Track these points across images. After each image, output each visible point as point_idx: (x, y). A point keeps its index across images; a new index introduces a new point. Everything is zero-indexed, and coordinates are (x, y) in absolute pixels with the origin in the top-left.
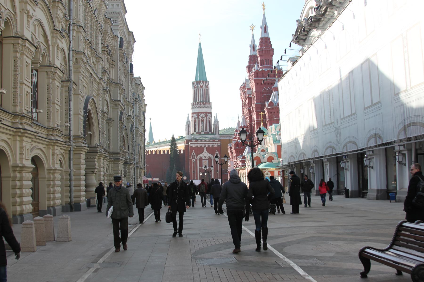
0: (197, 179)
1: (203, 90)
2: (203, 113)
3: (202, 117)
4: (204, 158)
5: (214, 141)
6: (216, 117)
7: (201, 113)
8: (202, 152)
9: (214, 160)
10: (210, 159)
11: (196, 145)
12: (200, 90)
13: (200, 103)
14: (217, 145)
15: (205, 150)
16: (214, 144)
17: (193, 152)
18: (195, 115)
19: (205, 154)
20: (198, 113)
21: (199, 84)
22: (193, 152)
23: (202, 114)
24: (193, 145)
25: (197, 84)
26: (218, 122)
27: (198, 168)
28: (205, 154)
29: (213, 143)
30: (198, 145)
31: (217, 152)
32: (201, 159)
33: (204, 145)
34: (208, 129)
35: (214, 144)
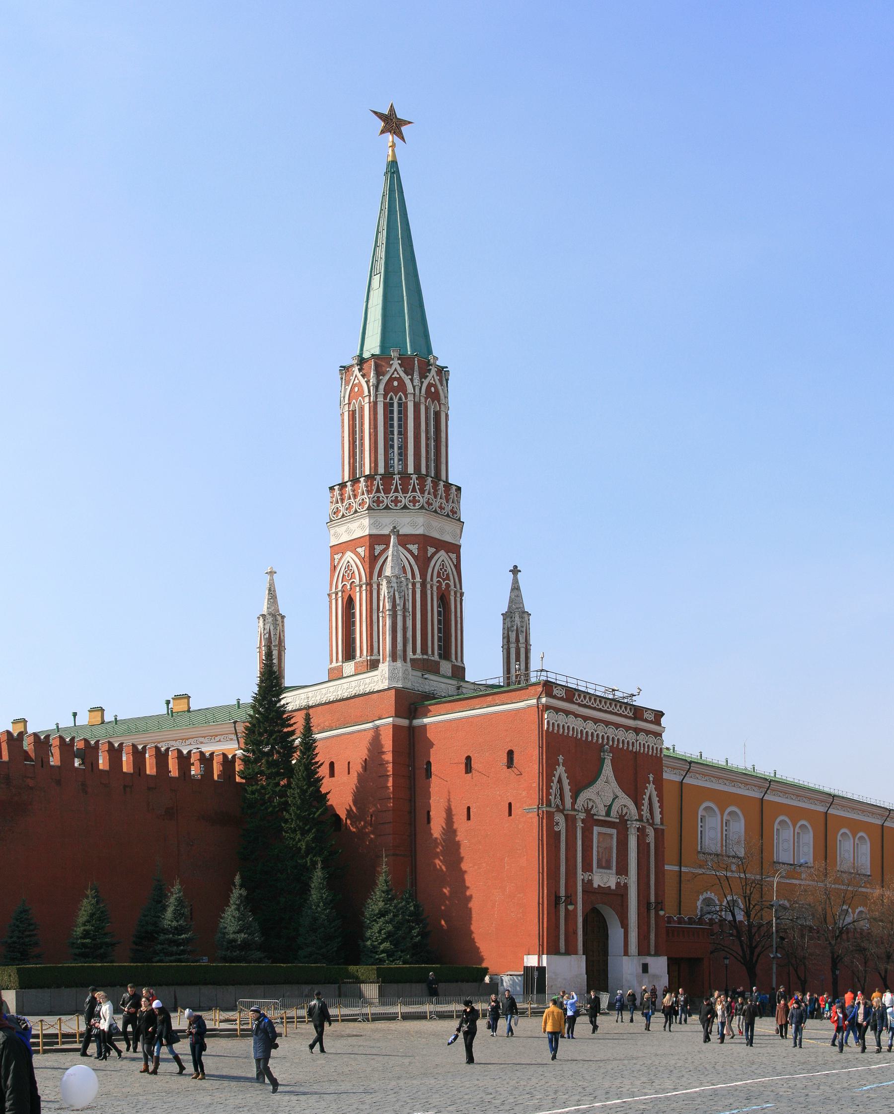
1: (437, 415)
6: (516, 588)
7: (440, 545)
10: (622, 825)
11: (572, 722)
12: (427, 409)
16: (642, 737)
17: (560, 770)
19: (605, 793)
20: (425, 541)
21: (423, 376)
22: (560, 770)
23: (442, 553)
24: (561, 719)
26: (524, 615)
27: (580, 875)
28: (605, 793)
29: (637, 731)
30: (578, 724)
31: (651, 787)
32: (591, 820)
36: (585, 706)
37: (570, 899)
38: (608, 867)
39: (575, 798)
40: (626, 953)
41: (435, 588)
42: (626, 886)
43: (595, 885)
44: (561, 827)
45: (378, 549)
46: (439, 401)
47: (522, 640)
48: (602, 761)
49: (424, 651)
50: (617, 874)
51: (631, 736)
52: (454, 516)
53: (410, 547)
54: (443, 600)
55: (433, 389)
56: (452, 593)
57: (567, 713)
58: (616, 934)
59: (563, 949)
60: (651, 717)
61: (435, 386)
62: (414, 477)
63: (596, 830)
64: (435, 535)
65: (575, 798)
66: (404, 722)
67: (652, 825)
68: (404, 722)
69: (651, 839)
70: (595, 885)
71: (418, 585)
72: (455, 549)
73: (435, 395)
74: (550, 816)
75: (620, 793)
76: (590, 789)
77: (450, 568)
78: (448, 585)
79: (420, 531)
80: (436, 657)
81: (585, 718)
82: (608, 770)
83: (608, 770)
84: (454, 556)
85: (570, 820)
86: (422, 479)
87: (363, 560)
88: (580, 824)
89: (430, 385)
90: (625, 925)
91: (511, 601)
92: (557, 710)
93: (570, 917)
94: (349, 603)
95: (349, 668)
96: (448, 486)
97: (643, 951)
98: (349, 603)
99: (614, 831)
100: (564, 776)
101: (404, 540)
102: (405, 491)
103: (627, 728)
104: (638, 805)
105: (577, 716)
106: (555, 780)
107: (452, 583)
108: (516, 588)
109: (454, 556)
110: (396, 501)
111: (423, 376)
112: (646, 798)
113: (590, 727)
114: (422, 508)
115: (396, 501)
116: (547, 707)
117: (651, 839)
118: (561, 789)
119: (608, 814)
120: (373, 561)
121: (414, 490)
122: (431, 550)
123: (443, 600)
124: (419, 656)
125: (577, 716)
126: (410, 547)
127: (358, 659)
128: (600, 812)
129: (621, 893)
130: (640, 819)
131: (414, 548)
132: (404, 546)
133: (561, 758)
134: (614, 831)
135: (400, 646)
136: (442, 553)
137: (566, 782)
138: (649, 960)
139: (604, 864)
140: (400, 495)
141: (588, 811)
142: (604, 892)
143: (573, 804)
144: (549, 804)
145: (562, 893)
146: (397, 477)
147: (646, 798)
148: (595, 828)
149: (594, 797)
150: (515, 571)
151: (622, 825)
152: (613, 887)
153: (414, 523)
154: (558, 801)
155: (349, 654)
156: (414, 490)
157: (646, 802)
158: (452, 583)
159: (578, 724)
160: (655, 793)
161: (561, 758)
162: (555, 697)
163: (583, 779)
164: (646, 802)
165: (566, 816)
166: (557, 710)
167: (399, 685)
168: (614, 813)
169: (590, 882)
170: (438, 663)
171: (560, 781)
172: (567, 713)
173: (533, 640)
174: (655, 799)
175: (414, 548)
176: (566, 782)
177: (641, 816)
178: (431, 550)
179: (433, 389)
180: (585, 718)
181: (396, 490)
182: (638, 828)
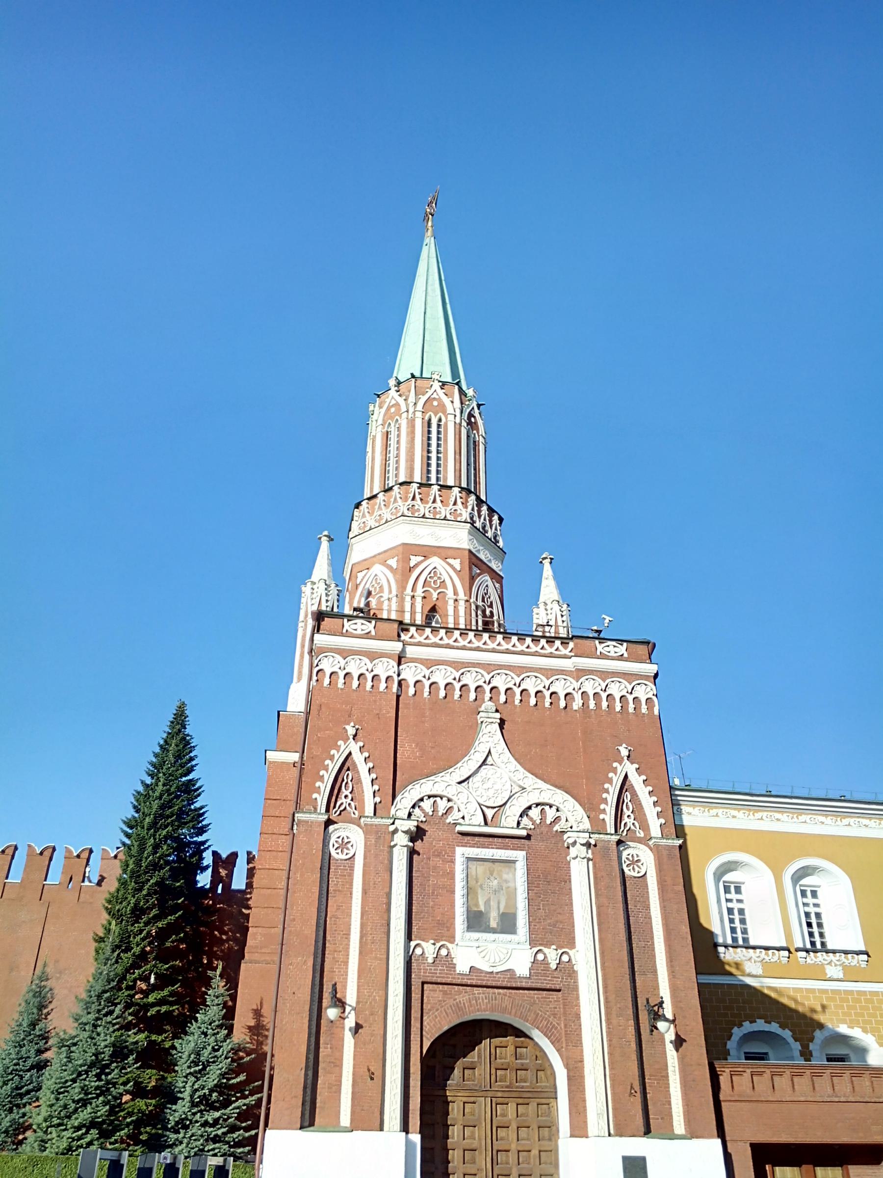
0: (368, 1118)
2: (444, 553)
3: (434, 580)
4: (475, 823)
5: (593, 655)
7: (426, 552)
8: (448, 743)
14: (617, 689)
15: (489, 737)
16: (590, 686)
18: (377, 569)
19: (489, 782)
23: (435, 561)
28: (489, 782)
35: (590, 686)
38: (508, 925)
40: (579, 1130)
41: (419, 600)
42: (567, 970)
43: (462, 967)
45: (360, 576)
46: (444, 411)
50: (532, 943)
53: (390, 562)
55: (435, 403)
56: (451, 602)
59: (345, 1119)
61: (439, 400)
63: (461, 853)
67: (645, 840)
70: (462, 967)
71: (394, 600)
75: (530, 781)
76: (437, 778)
84: (456, 563)
99: (520, 856)
101: (382, 558)
106: (333, 767)
107: (450, 593)
109: (456, 563)
118: (357, 781)
122: (414, 560)
129: (552, 987)
131: (393, 563)
132: (384, 563)
134: (520, 856)
139: (493, 924)
148: (459, 851)
158: (450, 593)
165: (368, 830)
169: (448, 962)
176: (363, 769)
178: (414, 560)
179: (435, 403)
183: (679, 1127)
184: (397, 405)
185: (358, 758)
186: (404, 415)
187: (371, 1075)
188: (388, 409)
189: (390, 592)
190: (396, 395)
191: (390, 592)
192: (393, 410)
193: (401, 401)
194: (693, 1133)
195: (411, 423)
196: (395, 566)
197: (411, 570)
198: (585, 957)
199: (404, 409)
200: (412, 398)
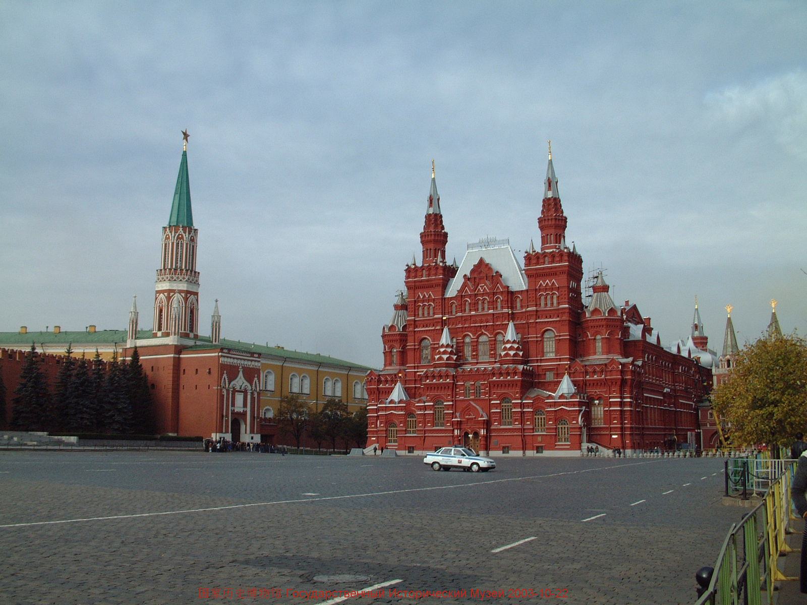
0: (227, 432)
1: (193, 246)
6: (217, 307)
9: (252, 394)
11: (229, 360)
13: (176, 270)
17: (225, 375)
19: (240, 381)
22: (225, 375)
24: (226, 359)
25: (185, 233)
28: (240, 381)
29: (252, 361)
32: (235, 391)
33: (239, 362)
34: (188, 327)
36: (234, 354)
37: (227, 416)
39: (229, 384)
40: (246, 433)
43: (236, 411)
44: (225, 393)
45: (171, 294)
46: (194, 241)
47: (218, 324)
48: (239, 371)
49: (185, 330)
51: (249, 363)
52: (196, 283)
54: (192, 312)
55: (192, 238)
57: (228, 357)
58: (243, 427)
60: (257, 356)
62: (184, 270)
64: (191, 290)
65: (229, 384)
66: (177, 356)
68: (177, 356)
69: (256, 396)
70: (236, 411)
71: (184, 308)
72: (196, 294)
73: (193, 240)
74: (221, 390)
75: (245, 381)
77: (195, 301)
78: (193, 307)
79: (185, 289)
80: (189, 332)
81: (234, 358)
82: (241, 374)
83: (241, 374)
84: (196, 296)
85: (228, 391)
86: (187, 271)
87: (166, 297)
88: (231, 392)
89: (192, 236)
90: (246, 425)
91: (215, 312)
92: (224, 357)
93: (227, 421)
94: (161, 311)
95: (159, 334)
96: (195, 272)
97: (252, 431)
98: (161, 311)
100: (226, 377)
101: (180, 292)
102: (181, 275)
103: (248, 360)
104: (251, 385)
105: (231, 358)
106: (223, 378)
108: (217, 307)
109: (196, 296)
110: (178, 278)
111: (189, 234)
112: (254, 382)
113: (235, 361)
114: (186, 281)
115: (178, 278)
116: (222, 356)
117: (256, 396)
119: (240, 388)
120: (169, 298)
121: (184, 275)
122: (189, 295)
123: (192, 312)
124: (183, 331)
125: (231, 358)
126: (182, 294)
127: (163, 331)
128: (238, 388)
129: (245, 413)
130: (252, 389)
131: (183, 295)
132: (180, 294)
133: (225, 372)
135: (177, 331)
136: (192, 296)
137: (226, 379)
138: (252, 435)
140: (179, 276)
141: (234, 388)
142: (239, 413)
143: (229, 386)
144: (221, 386)
145: (224, 414)
146: (179, 270)
147: (254, 382)
149: (236, 383)
150: (217, 301)
151: (245, 392)
152: (242, 412)
153: (183, 286)
154: (224, 385)
155: (160, 329)
156: (184, 275)
157: (254, 384)
159: (232, 360)
160: (257, 381)
161: (225, 372)
162: (224, 353)
163: (233, 376)
164: (254, 384)
165: (226, 390)
166: (224, 357)
167: (176, 344)
168: (242, 388)
169: (234, 410)
170: (189, 334)
171: (225, 379)
172: (228, 357)
173: (221, 325)
174: (257, 382)
175: (183, 295)
176: (226, 379)
177: (252, 389)
178: (189, 295)
180: (234, 358)
181: (178, 274)
182: (251, 393)
183: (255, 432)
184: (182, 235)
185: (226, 377)
186: (185, 241)
187: (227, 426)
188: (179, 235)
189: (182, 304)
190: (182, 231)
191: (182, 304)
192: (180, 236)
193: (184, 235)
194: (257, 434)
195: (187, 244)
196: (184, 296)
197: (188, 298)
198: (248, 409)
199: (185, 239)
200: (187, 236)
